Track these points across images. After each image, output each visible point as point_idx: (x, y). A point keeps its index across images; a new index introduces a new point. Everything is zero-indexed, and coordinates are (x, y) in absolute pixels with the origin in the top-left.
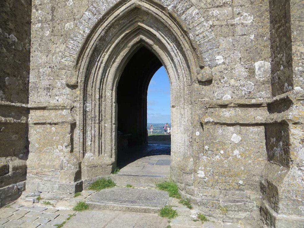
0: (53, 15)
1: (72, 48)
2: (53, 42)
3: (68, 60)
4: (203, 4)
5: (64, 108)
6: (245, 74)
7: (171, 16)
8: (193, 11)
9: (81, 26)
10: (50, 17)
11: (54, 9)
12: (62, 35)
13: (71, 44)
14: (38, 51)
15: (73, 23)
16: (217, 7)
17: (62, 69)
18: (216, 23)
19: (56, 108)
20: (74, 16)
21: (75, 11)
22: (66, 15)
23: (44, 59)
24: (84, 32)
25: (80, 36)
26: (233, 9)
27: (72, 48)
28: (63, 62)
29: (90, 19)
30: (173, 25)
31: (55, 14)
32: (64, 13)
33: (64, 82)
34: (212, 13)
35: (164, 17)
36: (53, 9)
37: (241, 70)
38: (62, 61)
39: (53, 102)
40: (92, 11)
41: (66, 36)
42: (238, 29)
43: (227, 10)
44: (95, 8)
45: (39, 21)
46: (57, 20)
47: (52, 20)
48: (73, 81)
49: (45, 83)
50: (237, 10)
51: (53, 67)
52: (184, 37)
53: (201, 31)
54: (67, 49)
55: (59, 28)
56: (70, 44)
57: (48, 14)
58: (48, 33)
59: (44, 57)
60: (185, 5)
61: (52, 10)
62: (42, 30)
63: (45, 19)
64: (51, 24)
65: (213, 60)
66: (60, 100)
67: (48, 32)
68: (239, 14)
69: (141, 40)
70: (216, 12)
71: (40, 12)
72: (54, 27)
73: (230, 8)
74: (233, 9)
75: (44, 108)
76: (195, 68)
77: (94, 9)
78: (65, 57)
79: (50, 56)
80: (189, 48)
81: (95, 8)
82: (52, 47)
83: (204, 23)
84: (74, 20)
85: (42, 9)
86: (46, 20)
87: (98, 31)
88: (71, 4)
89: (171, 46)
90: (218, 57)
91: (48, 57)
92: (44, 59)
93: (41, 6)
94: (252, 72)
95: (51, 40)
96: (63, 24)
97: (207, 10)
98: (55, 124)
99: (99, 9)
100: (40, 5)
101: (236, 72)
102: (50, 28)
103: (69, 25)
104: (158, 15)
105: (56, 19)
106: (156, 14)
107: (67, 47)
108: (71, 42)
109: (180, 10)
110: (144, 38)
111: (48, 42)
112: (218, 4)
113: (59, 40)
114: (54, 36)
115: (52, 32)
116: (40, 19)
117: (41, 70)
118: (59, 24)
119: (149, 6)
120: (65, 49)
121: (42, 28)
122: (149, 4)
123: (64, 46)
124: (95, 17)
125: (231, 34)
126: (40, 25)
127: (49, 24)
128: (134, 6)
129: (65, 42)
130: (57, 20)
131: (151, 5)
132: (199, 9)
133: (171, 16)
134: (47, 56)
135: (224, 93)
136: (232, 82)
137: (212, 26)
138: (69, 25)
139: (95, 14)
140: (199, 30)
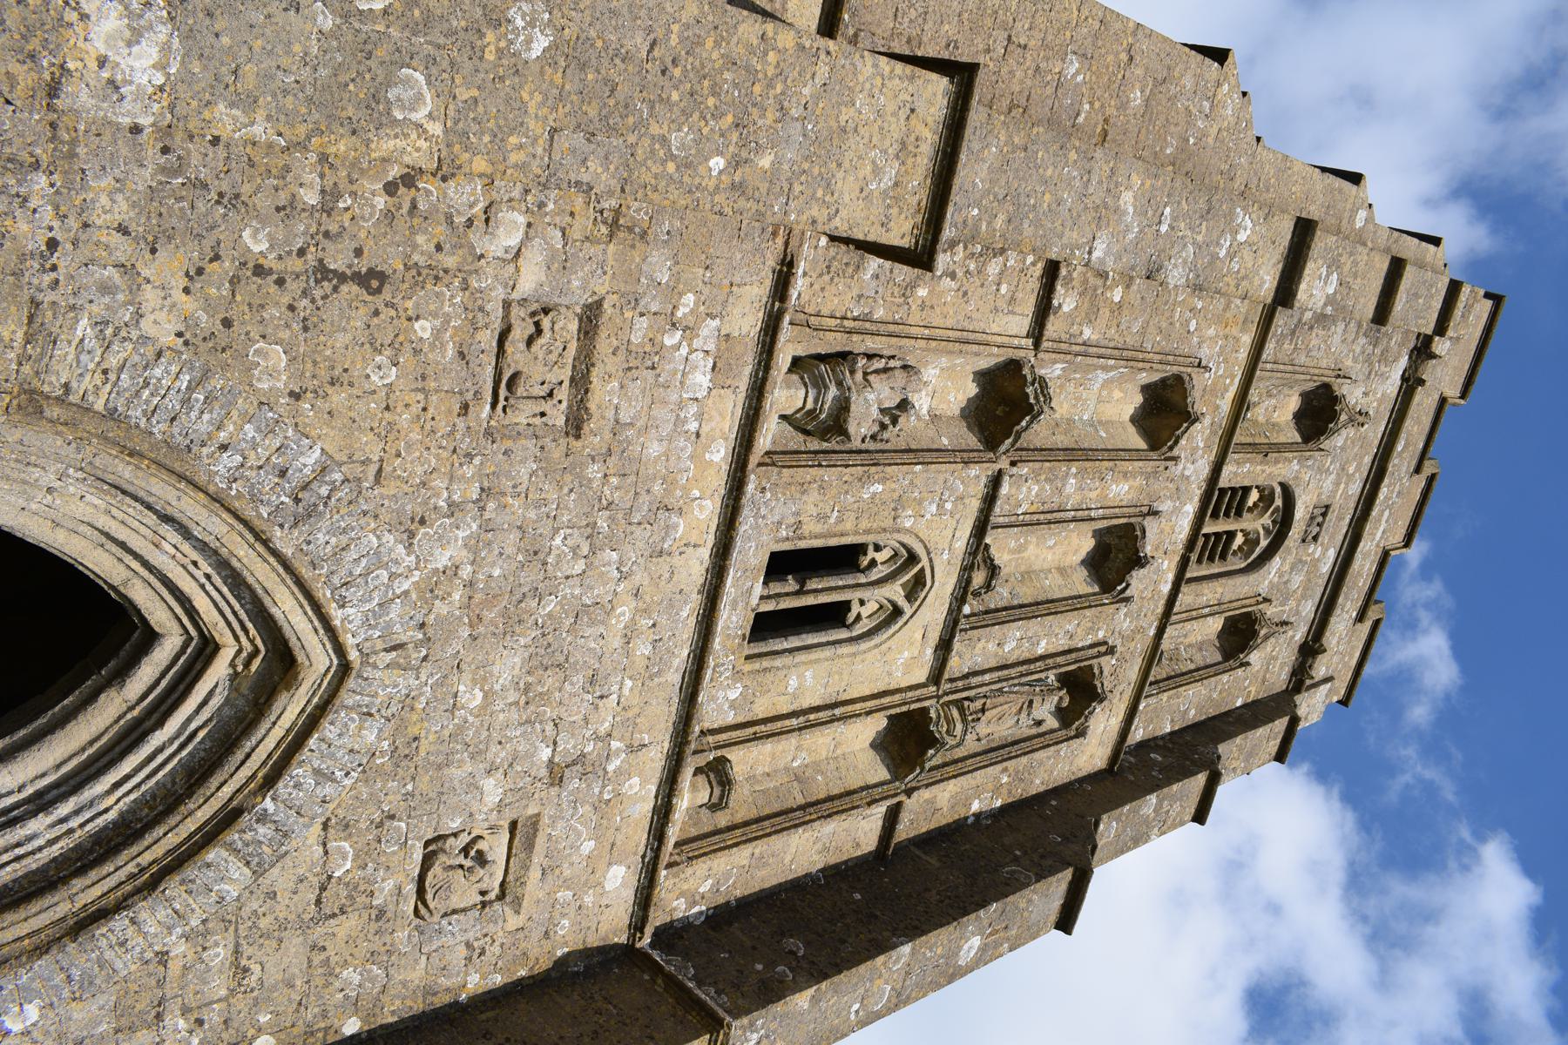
0: (342, 278)
1: (146, 384)
2: (200, 271)
3: (84, 358)
4: (255, 906)
7: (229, 817)
9: (258, 430)
10: (338, 261)
11: (375, 284)
12: (227, 323)
14: (163, 170)
15: (280, 385)
16: (237, 952)
17: (31, 318)
18: (175, 967)
20: (316, 392)
21: (338, 397)
22: (328, 353)
24: (224, 447)
25: (204, 426)
26: (219, 1000)
27: (146, 384)
28: (73, 328)
29: (283, 473)
30: (191, 825)
31: (344, 288)
32: (342, 339)
34: (217, 944)
35: (227, 790)
36: (372, 280)
38: (84, 322)
40: (315, 485)
44: (329, 497)
45: (330, 196)
46: (313, 301)
47: (323, 272)
50: (213, 1016)
51: (54, 268)
52: (132, 877)
54: (150, 352)
55: (272, 312)
56: (174, 369)
57: (358, 252)
58: (256, 244)
59: (122, 210)
60: (265, 848)
61: (372, 273)
62: (278, 209)
63: (333, 228)
64: (297, 264)
67: (259, 247)
68: (200, 1022)
69: (150, 637)
70: (219, 954)
71: (381, 202)
72: (280, 282)
73: (223, 992)
74: (219, 1000)
77: (324, 491)
78: (101, 336)
79: (123, 248)
80: (78, 905)
81: (329, 497)
82: (168, 267)
83: (179, 930)
84: (292, 394)
85: (389, 215)
86: (327, 234)
87: (214, 519)
88: (374, 378)
89: (108, 799)
90: (33, 1012)
91: (116, 238)
93: (405, 210)
95: (216, 258)
96: (285, 335)
99: (321, 514)
100: (414, 206)
102: (280, 258)
103: (273, 366)
104: (243, 763)
105: (318, 293)
106: (248, 756)
107: (159, 355)
108: (186, 378)
109: (248, 836)
110: (161, 655)
111: (208, 243)
112: (247, 950)
113: (208, 306)
114: (235, 281)
115: (259, 271)
116: (341, 205)
117: (42, 180)
118: (291, 308)
119: (287, 726)
120: (145, 339)
122: (294, 724)
123: (168, 339)
124: (287, 500)
125: (124, 1022)
126: (311, 198)
127: (302, 252)
128: (301, 657)
129: (186, 343)
130: (313, 301)
131: (288, 731)
132: (238, 899)
133: (229, 817)
134: (123, 230)
139: (297, 500)
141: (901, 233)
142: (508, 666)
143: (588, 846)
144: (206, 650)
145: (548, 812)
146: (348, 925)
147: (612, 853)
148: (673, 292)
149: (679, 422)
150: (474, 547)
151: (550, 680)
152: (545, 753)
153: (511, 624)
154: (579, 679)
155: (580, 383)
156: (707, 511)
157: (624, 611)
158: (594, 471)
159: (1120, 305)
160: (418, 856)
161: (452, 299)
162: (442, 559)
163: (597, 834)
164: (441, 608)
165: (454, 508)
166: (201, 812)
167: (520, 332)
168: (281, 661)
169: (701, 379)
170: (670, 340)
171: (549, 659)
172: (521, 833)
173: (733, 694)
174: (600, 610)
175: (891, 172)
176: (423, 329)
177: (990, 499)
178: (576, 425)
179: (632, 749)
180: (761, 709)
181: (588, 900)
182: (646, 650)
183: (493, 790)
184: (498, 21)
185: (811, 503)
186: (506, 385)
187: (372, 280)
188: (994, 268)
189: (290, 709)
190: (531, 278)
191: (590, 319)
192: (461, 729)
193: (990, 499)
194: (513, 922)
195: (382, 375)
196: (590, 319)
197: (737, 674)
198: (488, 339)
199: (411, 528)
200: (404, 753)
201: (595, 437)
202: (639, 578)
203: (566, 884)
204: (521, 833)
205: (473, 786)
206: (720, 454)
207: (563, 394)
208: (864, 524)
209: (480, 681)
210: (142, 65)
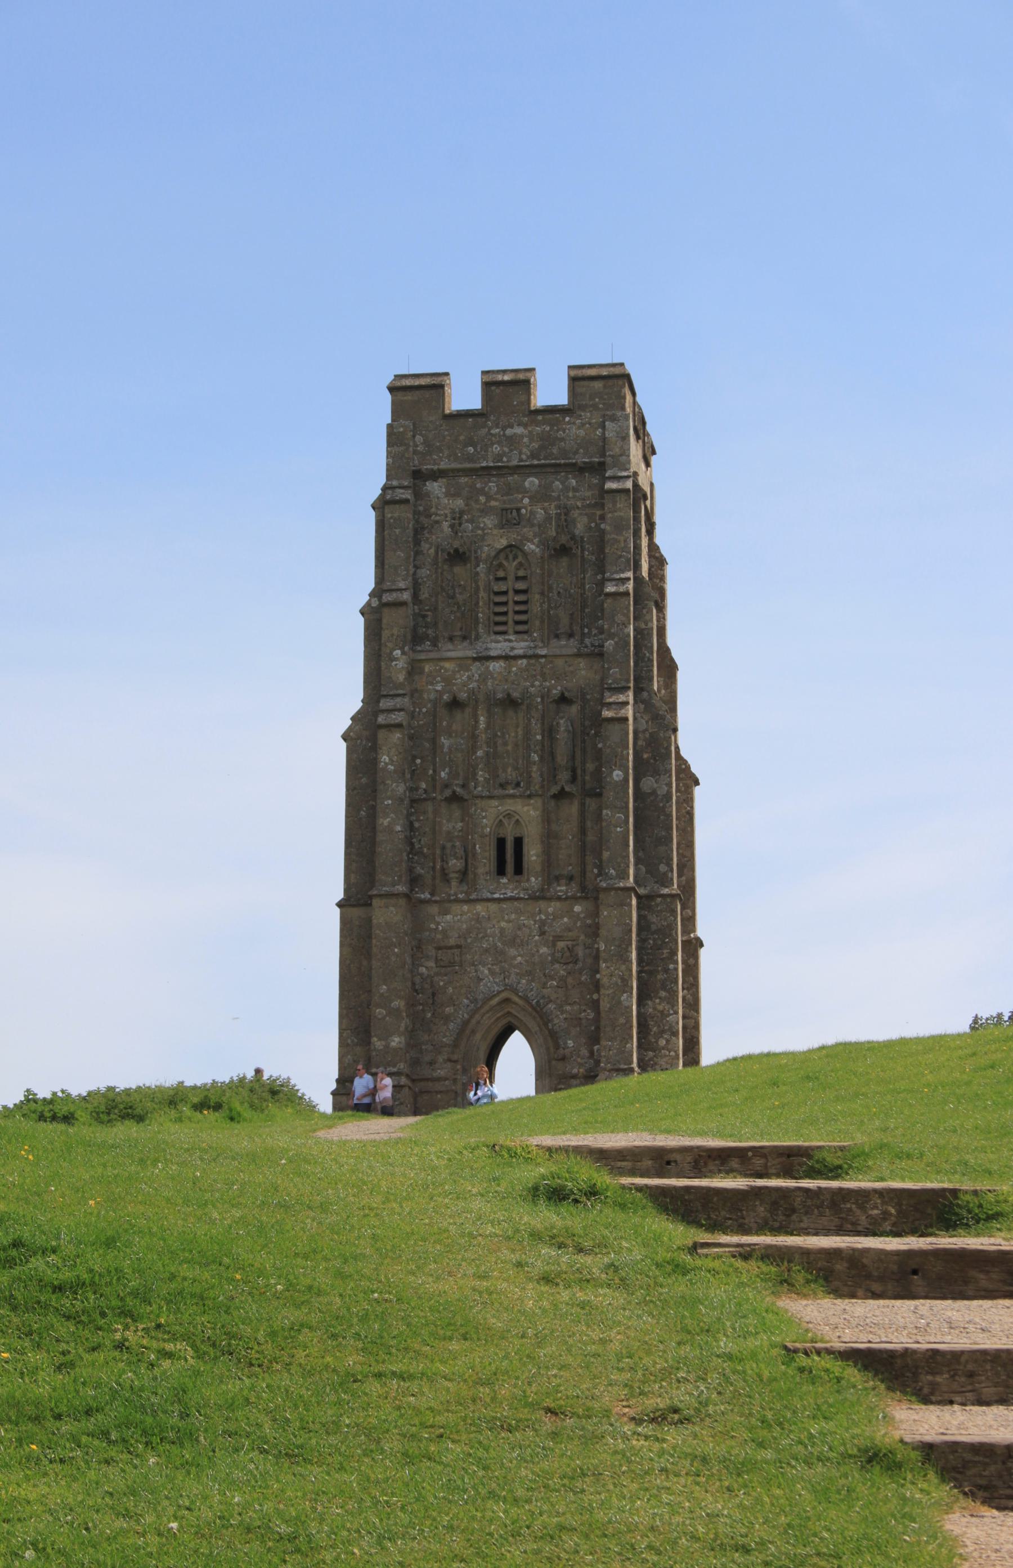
5: (446, 1079)
6: (587, 1054)
8: (551, 1006)
10: (431, 1001)
13: (451, 1026)
19: (438, 1079)
23: (426, 1037)
25: (459, 1020)
33: (446, 1057)
36: (434, 994)
37: (584, 1052)
39: (435, 1075)
41: (447, 1019)
42: (584, 1021)
43: (576, 1007)
45: (421, 1004)
47: (433, 1003)
48: (455, 1057)
49: (427, 1058)
50: (583, 1008)
53: (559, 1021)
58: (429, 1015)
65: (566, 1043)
66: (440, 1073)
70: (568, 1008)
75: (428, 1080)
76: (552, 1050)
92: (426, 1037)
94: (592, 1053)
97: (561, 1006)
98: (441, 1092)
101: (581, 1053)
103: (449, 1010)
110: (513, 1021)
121: (423, 1010)
135: (573, 1068)
136: (579, 1060)
137: (565, 1019)
138: (449, 1010)
140: (556, 1021)
141: (402, 902)
142: (513, 952)
143: (566, 920)
144: (509, 1013)
145: (552, 933)
146: (570, 980)
147: (570, 912)
148: (431, 930)
149: (458, 921)
150: (484, 966)
151: (518, 941)
152: (537, 938)
153: (502, 953)
154: (519, 933)
155: (451, 948)
156: (479, 907)
157: (503, 924)
158: (469, 940)
159: (421, 758)
160: (557, 966)
161: (436, 979)
162: (486, 972)
163: (562, 917)
164: (497, 970)
165: (476, 971)
166: (534, 1013)
167: (442, 964)
168: (507, 1000)
169: (449, 917)
170: (440, 928)
171: (513, 942)
172: (558, 938)
173: (533, 879)
174: (502, 930)
175: (392, 909)
176: (441, 984)
177: (482, 797)
178: (459, 947)
179: (540, 912)
180: (538, 868)
181: (582, 916)
182: (513, 916)
183: (544, 950)
184: (382, 995)
185: (481, 870)
186: (452, 964)
187: (434, 994)
188: (417, 825)
189: (516, 999)
190: (431, 964)
191: (439, 948)
192: (527, 961)
193: (482, 797)
194: (582, 937)
195: (451, 990)
196: (439, 948)
197: (528, 880)
198: (443, 970)
199: (480, 980)
200: (529, 973)
201: (462, 942)
202: (494, 922)
203: (575, 923)
204: (558, 938)
205: (541, 955)
206: (465, 908)
207: (453, 951)
208: (488, 848)
209: (515, 958)
210: (397, 1039)
